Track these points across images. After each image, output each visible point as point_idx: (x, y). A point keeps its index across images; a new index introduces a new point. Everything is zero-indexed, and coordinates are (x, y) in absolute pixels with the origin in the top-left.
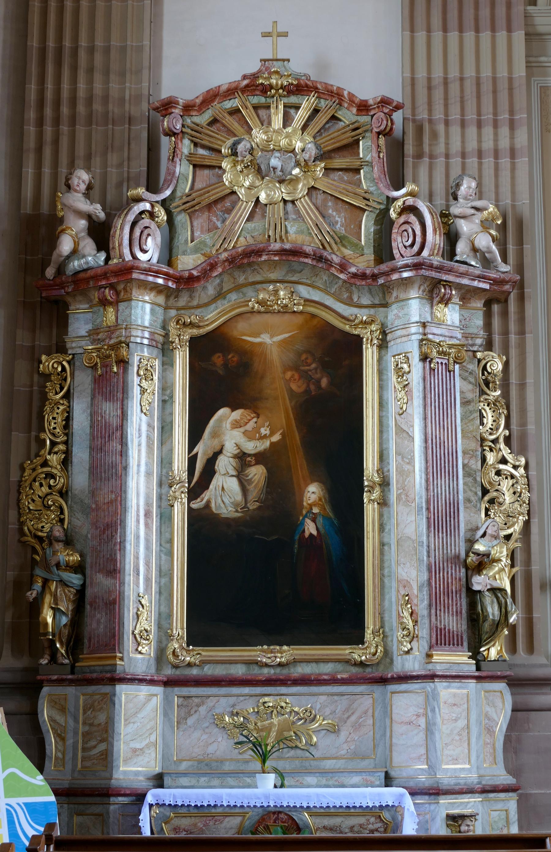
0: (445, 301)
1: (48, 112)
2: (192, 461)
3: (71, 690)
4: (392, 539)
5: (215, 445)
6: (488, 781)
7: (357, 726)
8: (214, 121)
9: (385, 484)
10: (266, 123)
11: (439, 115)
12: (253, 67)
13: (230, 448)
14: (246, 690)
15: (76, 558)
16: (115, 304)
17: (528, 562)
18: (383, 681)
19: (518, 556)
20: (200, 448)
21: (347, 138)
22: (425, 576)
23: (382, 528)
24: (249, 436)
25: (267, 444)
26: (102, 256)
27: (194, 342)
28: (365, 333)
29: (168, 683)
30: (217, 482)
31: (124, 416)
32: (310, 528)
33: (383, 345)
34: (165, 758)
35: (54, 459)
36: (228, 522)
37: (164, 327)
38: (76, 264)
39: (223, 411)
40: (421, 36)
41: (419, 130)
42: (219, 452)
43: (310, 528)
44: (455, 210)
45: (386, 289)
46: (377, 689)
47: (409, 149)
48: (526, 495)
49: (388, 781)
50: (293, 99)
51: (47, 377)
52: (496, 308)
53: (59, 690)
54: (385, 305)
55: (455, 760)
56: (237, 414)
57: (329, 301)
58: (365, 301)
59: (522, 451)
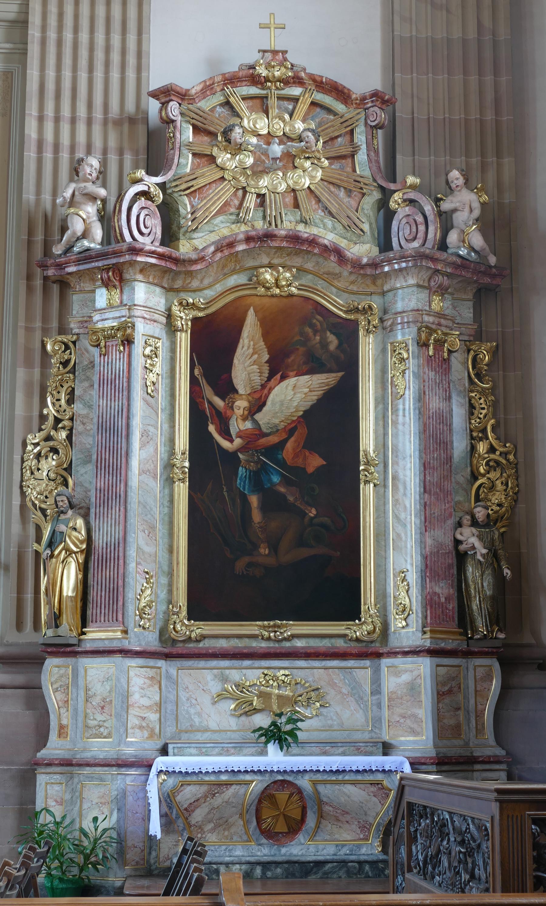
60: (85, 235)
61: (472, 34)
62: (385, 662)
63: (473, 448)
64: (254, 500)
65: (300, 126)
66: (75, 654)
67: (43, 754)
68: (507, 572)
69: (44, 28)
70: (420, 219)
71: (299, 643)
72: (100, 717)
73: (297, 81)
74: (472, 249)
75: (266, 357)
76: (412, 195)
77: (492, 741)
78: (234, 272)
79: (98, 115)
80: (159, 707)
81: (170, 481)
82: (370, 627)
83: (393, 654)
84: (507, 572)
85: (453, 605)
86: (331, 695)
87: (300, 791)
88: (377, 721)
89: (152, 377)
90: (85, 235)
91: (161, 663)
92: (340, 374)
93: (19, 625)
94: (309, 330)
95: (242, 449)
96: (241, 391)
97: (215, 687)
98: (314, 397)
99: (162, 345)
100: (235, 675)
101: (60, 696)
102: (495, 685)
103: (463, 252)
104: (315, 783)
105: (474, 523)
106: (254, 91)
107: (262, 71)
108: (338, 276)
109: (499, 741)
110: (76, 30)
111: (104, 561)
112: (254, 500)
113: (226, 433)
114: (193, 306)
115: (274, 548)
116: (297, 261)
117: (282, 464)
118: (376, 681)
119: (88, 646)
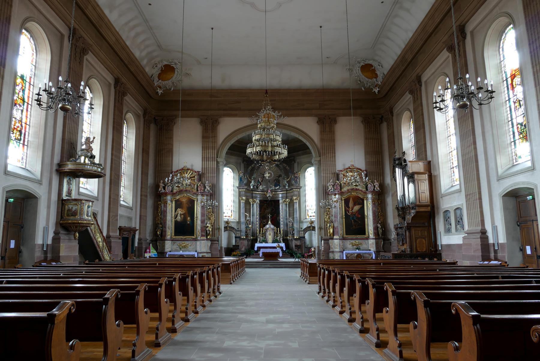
0: (204, 196)
2: (175, 215)
3: (161, 241)
4: (197, 224)
5: (178, 213)
6: (207, 252)
7: (193, 245)
9: (197, 217)
11: (205, 172)
13: (179, 213)
14: (181, 241)
15: (161, 226)
16: (166, 197)
18: (196, 240)
19: (213, 226)
20: (176, 213)
21: (194, 176)
22: (200, 229)
23: (196, 223)
24: (182, 212)
25: (183, 213)
26: (164, 191)
28: (195, 199)
29: (172, 240)
31: (167, 209)
32: (188, 223)
33: (197, 201)
34: (172, 249)
35: (160, 214)
36: (179, 222)
37: (172, 199)
38: (161, 192)
41: (203, 174)
42: (178, 214)
43: (188, 223)
44: (206, 185)
45: (197, 194)
46: (196, 241)
47: (202, 176)
48: (214, 218)
49: (196, 251)
50: (187, 171)
51: (159, 204)
52: (212, 196)
53: (159, 241)
54: (197, 196)
55: (203, 249)
56: (180, 209)
57: (191, 196)
58: (195, 196)
60: (331, 189)
61: (376, 160)
62: (369, 240)
63: (378, 214)
64: (353, 221)
66: (333, 239)
67: (330, 251)
68: (383, 229)
69: (323, 162)
70: (371, 186)
71: (359, 238)
72: (337, 247)
74: (378, 190)
75: (353, 203)
76: (370, 183)
77: (382, 249)
78: (349, 193)
79: (330, 173)
80: (343, 245)
82: (367, 236)
83: (370, 239)
84: (383, 229)
85: (377, 233)
86: (363, 244)
87: (361, 255)
88: (368, 247)
89: (340, 206)
91: (342, 240)
92: (362, 205)
93: (325, 236)
94: (358, 200)
95: (351, 215)
96: (350, 207)
97: (349, 243)
98: (359, 208)
100: (351, 242)
101: (331, 244)
103: (377, 190)
104: (363, 254)
105: (379, 223)
106: (350, 170)
107: (351, 168)
108: (361, 193)
109: (383, 249)
110: (327, 162)
111: (335, 229)
112: (353, 221)
113: (349, 213)
114: (344, 197)
115: (355, 227)
116: (356, 191)
117: (356, 216)
118: (368, 242)
119: (335, 238)
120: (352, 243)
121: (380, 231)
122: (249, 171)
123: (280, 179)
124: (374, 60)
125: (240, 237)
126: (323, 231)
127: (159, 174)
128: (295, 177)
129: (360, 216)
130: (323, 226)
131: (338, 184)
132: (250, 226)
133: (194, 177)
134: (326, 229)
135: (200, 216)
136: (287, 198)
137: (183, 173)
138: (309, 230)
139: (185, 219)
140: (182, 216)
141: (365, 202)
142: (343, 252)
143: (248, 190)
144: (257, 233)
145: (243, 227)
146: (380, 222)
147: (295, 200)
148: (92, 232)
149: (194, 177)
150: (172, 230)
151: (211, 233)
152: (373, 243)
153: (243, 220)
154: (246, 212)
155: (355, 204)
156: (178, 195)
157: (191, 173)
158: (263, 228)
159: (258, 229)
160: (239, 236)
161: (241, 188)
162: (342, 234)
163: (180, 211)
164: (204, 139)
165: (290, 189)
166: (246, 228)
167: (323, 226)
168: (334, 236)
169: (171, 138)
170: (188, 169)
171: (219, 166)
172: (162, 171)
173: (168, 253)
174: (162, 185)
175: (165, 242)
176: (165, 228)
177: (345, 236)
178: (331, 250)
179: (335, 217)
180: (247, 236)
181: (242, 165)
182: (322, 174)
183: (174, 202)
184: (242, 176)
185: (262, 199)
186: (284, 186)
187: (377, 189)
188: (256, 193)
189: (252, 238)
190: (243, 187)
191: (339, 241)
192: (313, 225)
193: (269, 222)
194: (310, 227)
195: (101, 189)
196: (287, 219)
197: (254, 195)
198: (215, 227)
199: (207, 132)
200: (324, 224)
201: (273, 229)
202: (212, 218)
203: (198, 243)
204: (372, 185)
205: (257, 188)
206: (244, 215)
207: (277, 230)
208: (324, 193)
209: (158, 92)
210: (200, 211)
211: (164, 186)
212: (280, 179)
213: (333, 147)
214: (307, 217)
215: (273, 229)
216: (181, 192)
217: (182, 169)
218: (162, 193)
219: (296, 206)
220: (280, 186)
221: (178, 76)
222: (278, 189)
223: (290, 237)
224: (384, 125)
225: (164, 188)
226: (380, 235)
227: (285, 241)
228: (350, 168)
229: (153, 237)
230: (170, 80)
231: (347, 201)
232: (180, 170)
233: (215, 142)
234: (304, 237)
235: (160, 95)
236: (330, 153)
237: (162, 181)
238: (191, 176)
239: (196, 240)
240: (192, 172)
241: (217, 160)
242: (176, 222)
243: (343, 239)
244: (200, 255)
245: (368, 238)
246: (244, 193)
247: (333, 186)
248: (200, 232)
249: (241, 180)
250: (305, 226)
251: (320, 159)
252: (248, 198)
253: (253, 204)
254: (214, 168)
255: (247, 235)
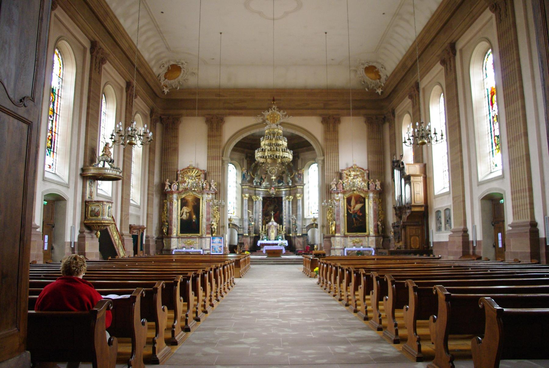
0: (209, 195)
1: (165, 170)
8: (184, 172)
9: (202, 216)
10: (190, 172)
11: (211, 171)
12: (188, 166)
13: (185, 211)
15: (167, 224)
17: (219, 224)
18: (201, 238)
20: (182, 211)
21: (199, 174)
23: (202, 220)
27: (181, 199)
28: (200, 198)
29: (178, 238)
30: (183, 215)
31: (173, 208)
32: (194, 221)
33: (203, 199)
34: (177, 246)
35: (165, 212)
38: (167, 190)
39: (184, 207)
40: (209, 161)
42: (183, 212)
43: (194, 221)
44: (211, 184)
45: (203, 193)
46: (201, 239)
47: (207, 175)
49: (201, 249)
51: (164, 203)
53: (166, 239)
56: (186, 207)
57: (197, 194)
59: (219, 211)
60: (334, 188)
63: (379, 212)
64: (354, 219)
65: (358, 173)
67: (332, 248)
68: (383, 227)
73: (358, 168)
77: (381, 246)
79: (334, 172)
81: (344, 217)
83: (370, 236)
88: (369, 244)
90: (334, 188)
93: (327, 233)
99: (343, 201)
102: (382, 240)
106: (352, 169)
112: (354, 219)
113: (350, 211)
115: (356, 224)
120: (353, 240)
121: (380, 229)
122: (252, 168)
123: (284, 175)
124: (377, 62)
125: (242, 235)
126: (325, 229)
127: (165, 173)
128: (299, 174)
129: (361, 214)
130: (325, 224)
131: (341, 183)
132: (253, 223)
133: (200, 175)
134: (328, 227)
135: (205, 214)
136: (290, 195)
137: (188, 172)
138: (312, 228)
139: (190, 217)
140: (188, 214)
141: (367, 200)
142: (344, 250)
143: (251, 187)
144: (259, 231)
145: (246, 224)
146: (380, 220)
147: (299, 197)
148: (111, 231)
149: (200, 175)
150: (177, 228)
151: (216, 231)
152: (372, 241)
153: (246, 217)
154: (248, 209)
155: (356, 203)
156: (184, 193)
157: (196, 172)
158: (265, 225)
159: (260, 226)
160: (242, 233)
161: (244, 185)
162: (343, 232)
163: (185, 209)
164: (210, 138)
165: (293, 186)
166: (249, 225)
167: (325, 224)
168: (335, 233)
169: (176, 137)
170: (194, 168)
171: (224, 165)
172: (168, 169)
173: (174, 251)
174: (168, 183)
175: (171, 240)
176: (171, 225)
177: (346, 233)
178: (333, 247)
179: (337, 215)
180: (249, 233)
181: (245, 161)
182: (326, 174)
183: (179, 201)
184: (245, 173)
185: (265, 196)
186: (288, 183)
187: (378, 188)
188: (259, 190)
189: (254, 235)
190: (246, 184)
191: (341, 239)
192: (316, 222)
193: (273, 220)
194: (312, 224)
195: (115, 191)
196: (289, 216)
197: (257, 192)
198: (220, 225)
199: (213, 131)
200: (326, 222)
201: (276, 227)
202: (218, 216)
203: (203, 240)
204: (374, 184)
205: (260, 184)
206: (247, 212)
207: (280, 227)
208: (326, 192)
209: (164, 91)
210: (205, 209)
211: (170, 184)
212: (284, 175)
213: (337, 147)
214: (310, 214)
215: (276, 227)
216: (186, 190)
217: (188, 168)
218: (169, 192)
219: (300, 203)
220: (283, 183)
221: (184, 75)
222: (281, 186)
223: (292, 234)
224: (387, 125)
225: (170, 186)
226: (380, 233)
227: (287, 238)
228: (352, 168)
229: (159, 234)
230: (176, 79)
231: (349, 200)
232: (186, 169)
233: (220, 140)
234: (307, 235)
235: (166, 94)
236: (334, 152)
237: (168, 180)
238: (197, 175)
239: (201, 237)
240: (197, 170)
241: (222, 159)
242: (182, 220)
243: (345, 236)
244: (206, 252)
245: (368, 236)
246: (247, 190)
247: (336, 185)
248: (205, 230)
249: (244, 177)
250: (308, 223)
251: (324, 158)
252: (251, 195)
253: (255, 201)
254: (219, 166)
255: (250, 232)
